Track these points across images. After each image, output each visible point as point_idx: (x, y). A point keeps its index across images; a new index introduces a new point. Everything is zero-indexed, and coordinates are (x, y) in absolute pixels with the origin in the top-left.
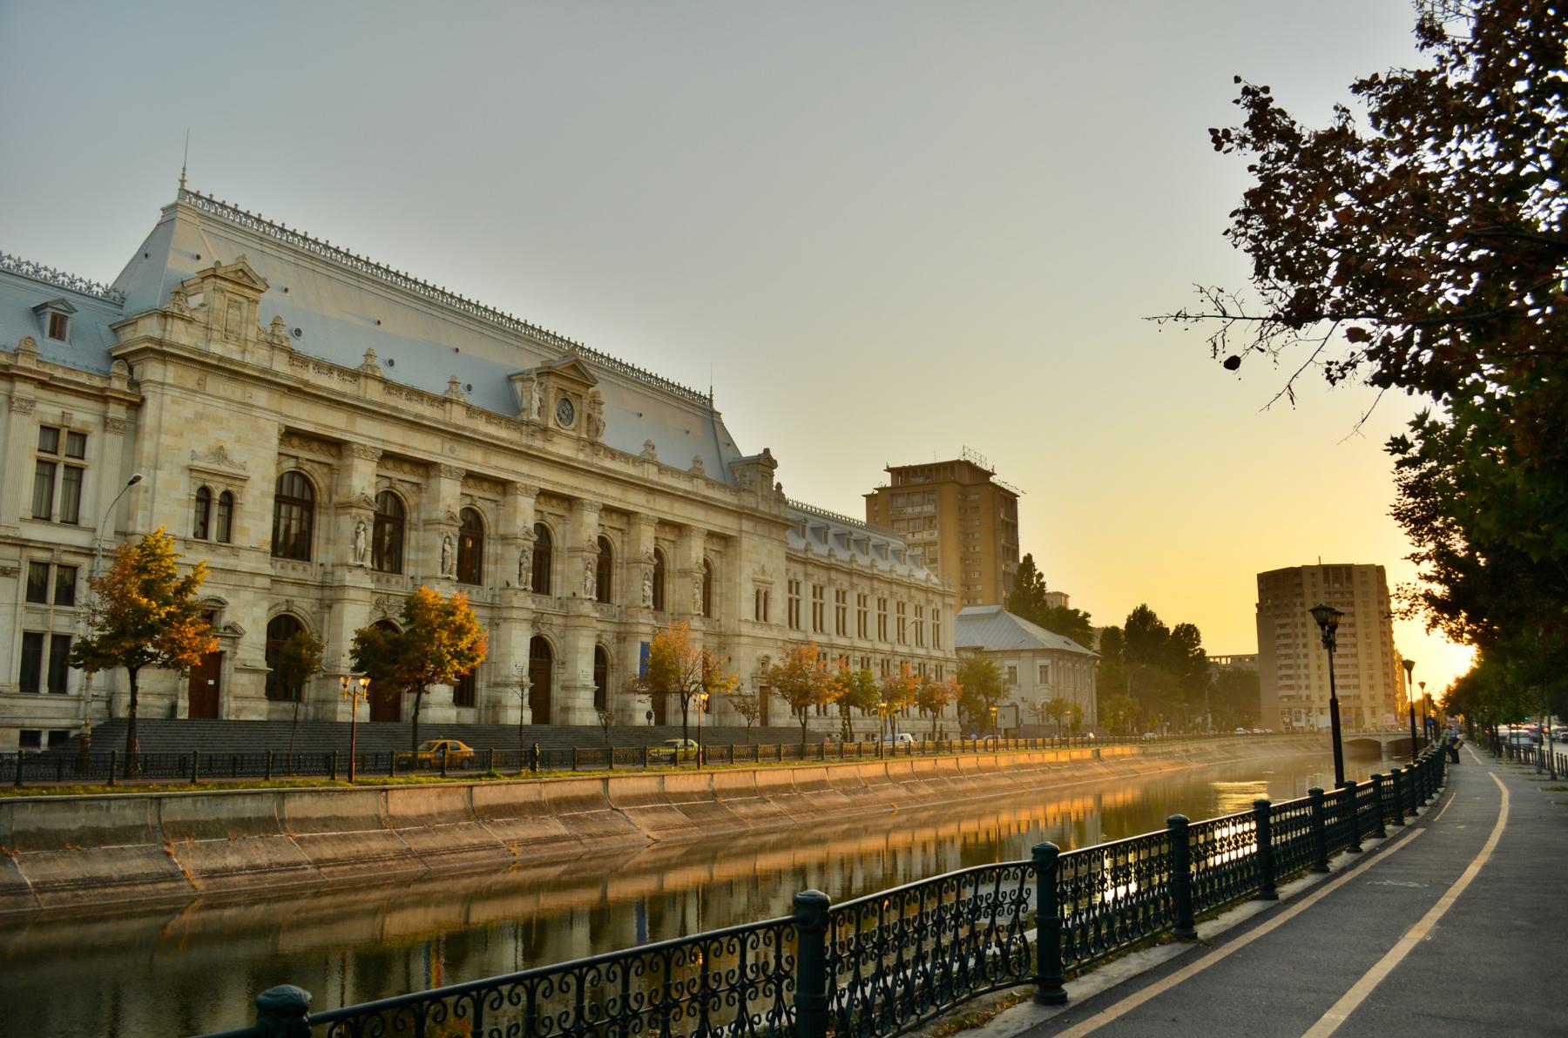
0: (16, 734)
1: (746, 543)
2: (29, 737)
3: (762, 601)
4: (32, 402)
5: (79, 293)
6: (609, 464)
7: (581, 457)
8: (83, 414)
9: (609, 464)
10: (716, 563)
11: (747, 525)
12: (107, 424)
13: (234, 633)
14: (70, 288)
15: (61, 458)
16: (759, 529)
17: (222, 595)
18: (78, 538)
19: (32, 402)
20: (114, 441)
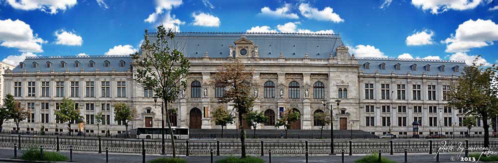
0: (117, 132)
1: (331, 75)
2: (119, 132)
3: (343, 91)
4: (114, 79)
5: (125, 57)
6: (262, 62)
7: (249, 62)
8: (124, 79)
9: (262, 62)
10: (325, 82)
11: (332, 70)
12: (128, 79)
13: (154, 114)
14: (123, 57)
15: (122, 86)
16: (340, 70)
17: (151, 106)
18: (125, 99)
19: (114, 79)
20: (129, 82)
